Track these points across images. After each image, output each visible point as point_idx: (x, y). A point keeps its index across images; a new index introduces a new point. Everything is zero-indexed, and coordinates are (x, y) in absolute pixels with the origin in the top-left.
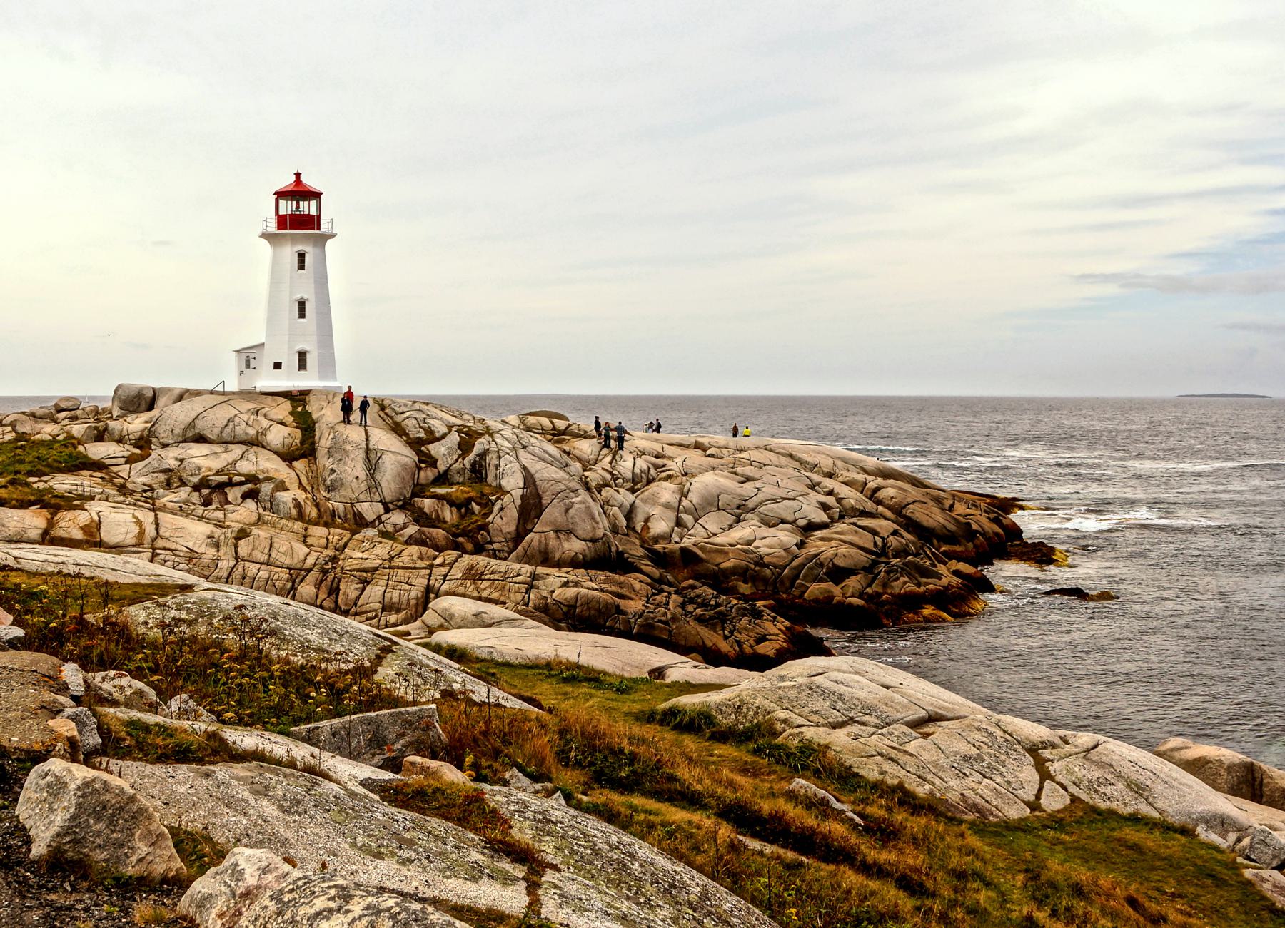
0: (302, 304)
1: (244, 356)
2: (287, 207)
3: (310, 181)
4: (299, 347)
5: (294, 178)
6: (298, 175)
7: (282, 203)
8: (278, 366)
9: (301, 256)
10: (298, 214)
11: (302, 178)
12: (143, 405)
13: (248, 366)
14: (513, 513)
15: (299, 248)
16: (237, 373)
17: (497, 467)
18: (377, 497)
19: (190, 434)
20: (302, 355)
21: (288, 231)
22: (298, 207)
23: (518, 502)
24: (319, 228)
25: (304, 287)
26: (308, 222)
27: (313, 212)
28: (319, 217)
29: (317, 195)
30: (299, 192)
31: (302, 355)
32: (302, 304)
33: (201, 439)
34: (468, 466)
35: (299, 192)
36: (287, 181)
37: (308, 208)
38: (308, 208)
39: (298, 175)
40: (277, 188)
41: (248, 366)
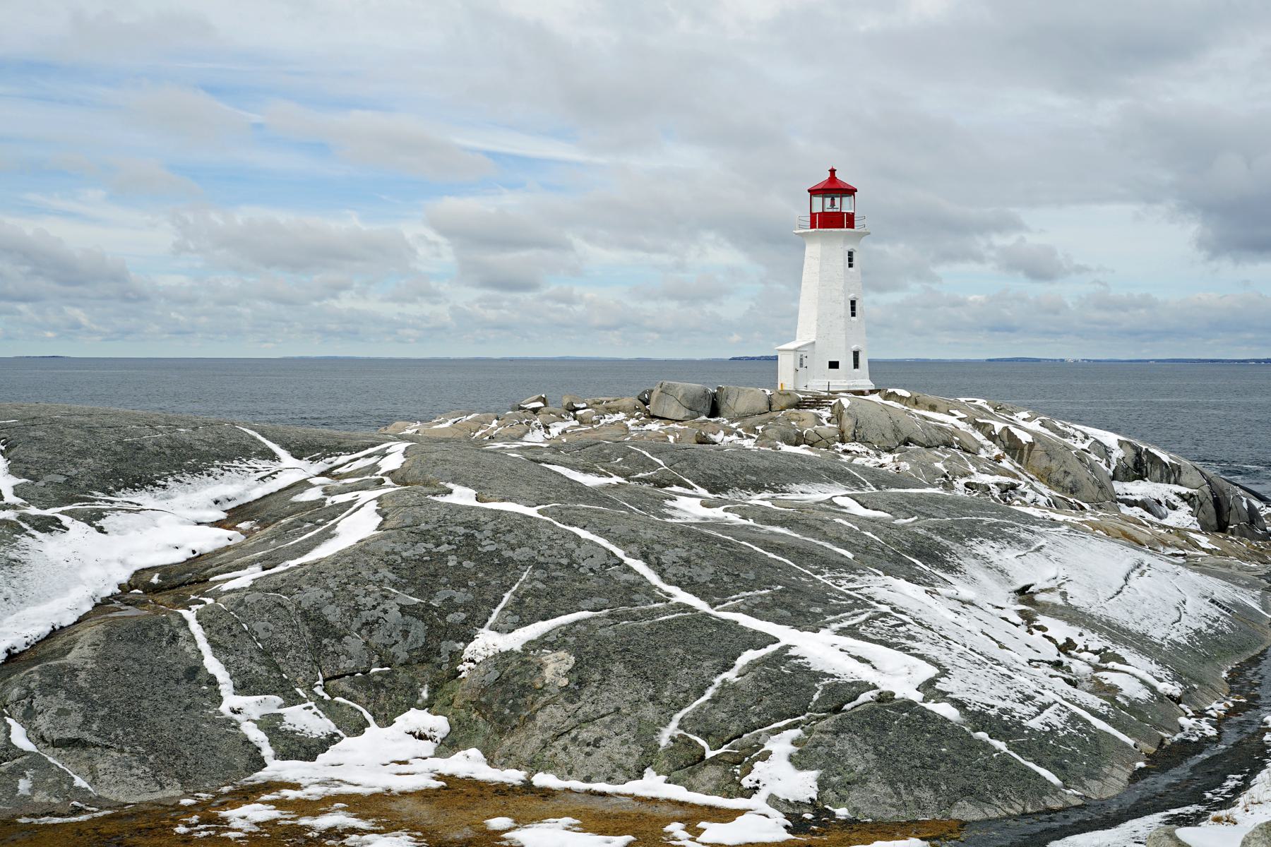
0: (853, 303)
2: (819, 204)
4: (854, 347)
5: (828, 175)
6: (833, 171)
7: (818, 201)
8: (834, 365)
9: (850, 254)
11: (837, 175)
13: (801, 365)
15: (849, 248)
16: (793, 372)
20: (856, 354)
22: (833, 204)
24: (851, 225)
26: (850, 220)
27: (847, 209)
30: (833, 188)
31: (856, 354)
32: (853, 303)
35: (833, 188)
37: (846, 205)
39: (833, 171)
41: (801, 365)
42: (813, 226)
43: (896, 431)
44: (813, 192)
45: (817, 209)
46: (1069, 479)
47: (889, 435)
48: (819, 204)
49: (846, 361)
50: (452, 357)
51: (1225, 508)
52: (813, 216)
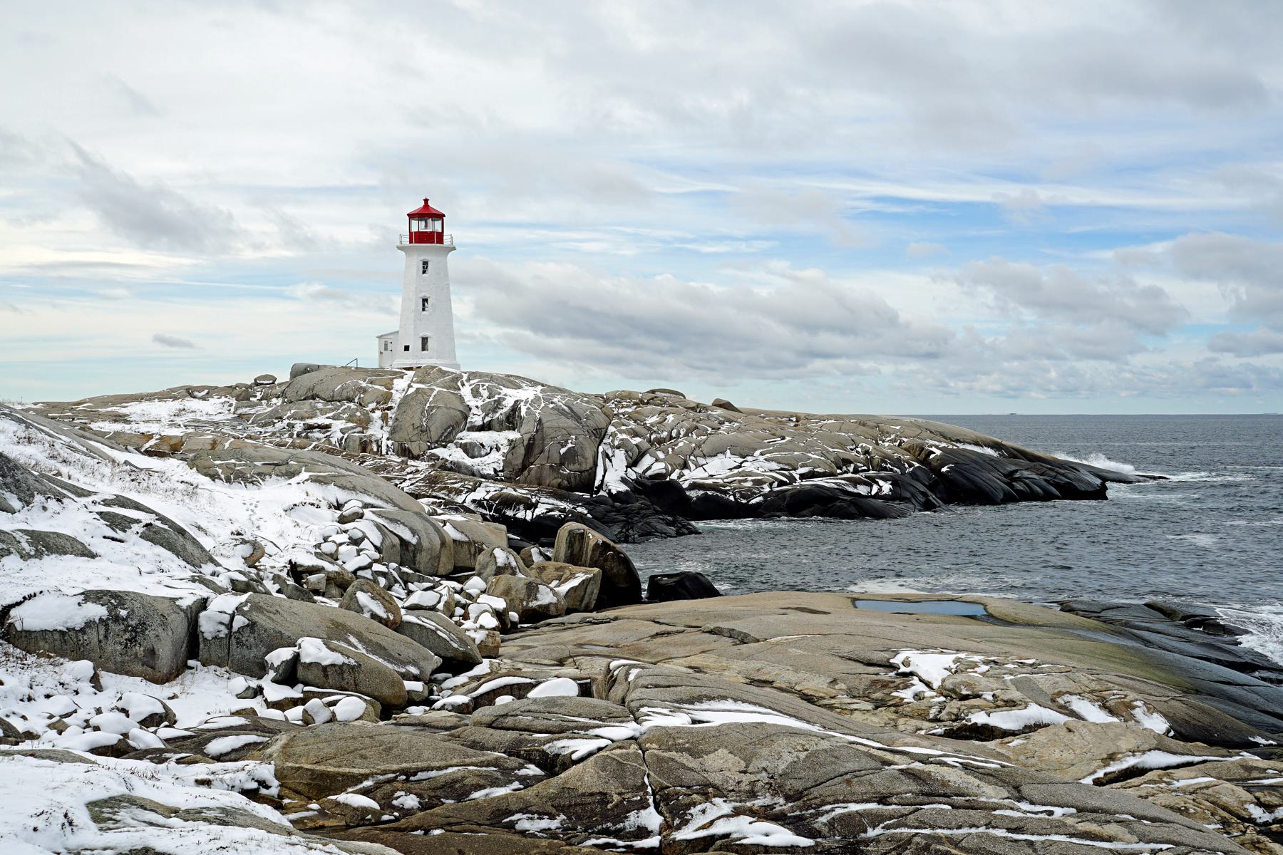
0: (425, 300)
1: (383, 341)
2: (417, 226)
6: (426, 201)
7: (415, 223)
9: (425, 263)
10: (427, 229)
13: (386, 349)
18: (425, 438)
20: (425, 340)
25: (427, 286)
29: (440, 216)
30: (426, 213)
31: (425, 340)
35: (426, 213)
36: (418, 205)
39: (426, 201)
41: (386, 349)
44: (411, 216)
45: (415, 229)
48: (417, 226)
49: (416, 345)
50: (1019, 413)
51: (536, 451)
52: (411, 233)
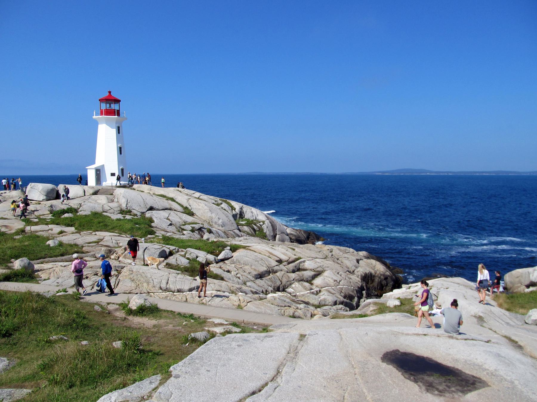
0: (120, 148)
3: (115, 95)
6: (110, 92)
7: (102, 104)
8: (113, 175)
12: (55, 195)
14: (271, 228)
17: (252, 212)
19: (148, 207)
21: (116, 117)
22: (110, 106)
23: (270, 224)
24: (118, 114)
28: (118, 112)
32: (120, 148)
33: (151, 209)
34: (239, 213)
38: (115, 107)
39: (110, 92)
40: (100, 98)
42: (102, 114)
43: (145, 204)
46: (221, 221)
47: (142, 206)
48: (104, 106)
